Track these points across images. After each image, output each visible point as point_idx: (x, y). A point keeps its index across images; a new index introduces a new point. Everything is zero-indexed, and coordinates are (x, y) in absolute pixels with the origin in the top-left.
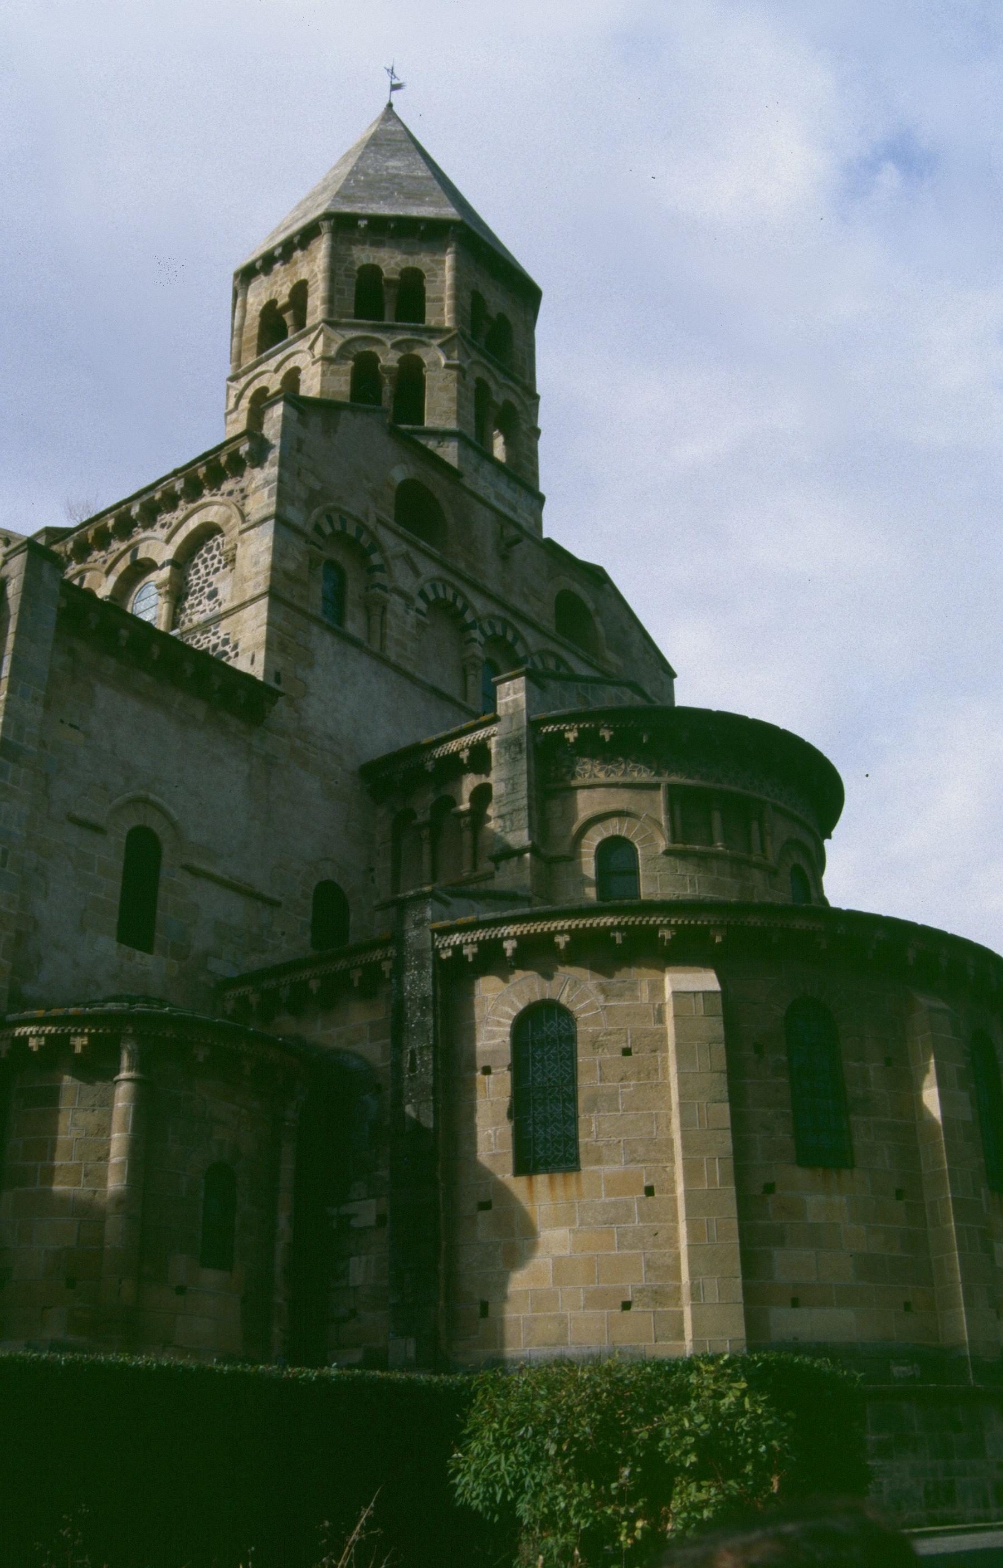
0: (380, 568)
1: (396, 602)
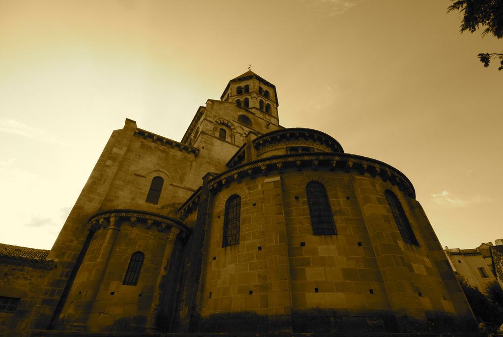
0: (234, 129)
1: (237, 135)
